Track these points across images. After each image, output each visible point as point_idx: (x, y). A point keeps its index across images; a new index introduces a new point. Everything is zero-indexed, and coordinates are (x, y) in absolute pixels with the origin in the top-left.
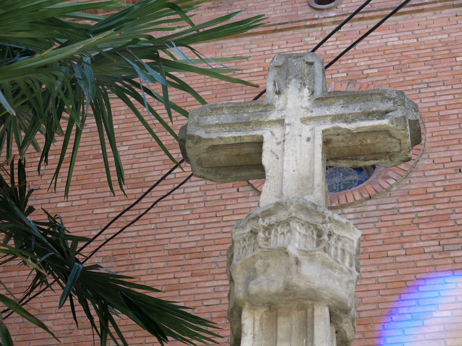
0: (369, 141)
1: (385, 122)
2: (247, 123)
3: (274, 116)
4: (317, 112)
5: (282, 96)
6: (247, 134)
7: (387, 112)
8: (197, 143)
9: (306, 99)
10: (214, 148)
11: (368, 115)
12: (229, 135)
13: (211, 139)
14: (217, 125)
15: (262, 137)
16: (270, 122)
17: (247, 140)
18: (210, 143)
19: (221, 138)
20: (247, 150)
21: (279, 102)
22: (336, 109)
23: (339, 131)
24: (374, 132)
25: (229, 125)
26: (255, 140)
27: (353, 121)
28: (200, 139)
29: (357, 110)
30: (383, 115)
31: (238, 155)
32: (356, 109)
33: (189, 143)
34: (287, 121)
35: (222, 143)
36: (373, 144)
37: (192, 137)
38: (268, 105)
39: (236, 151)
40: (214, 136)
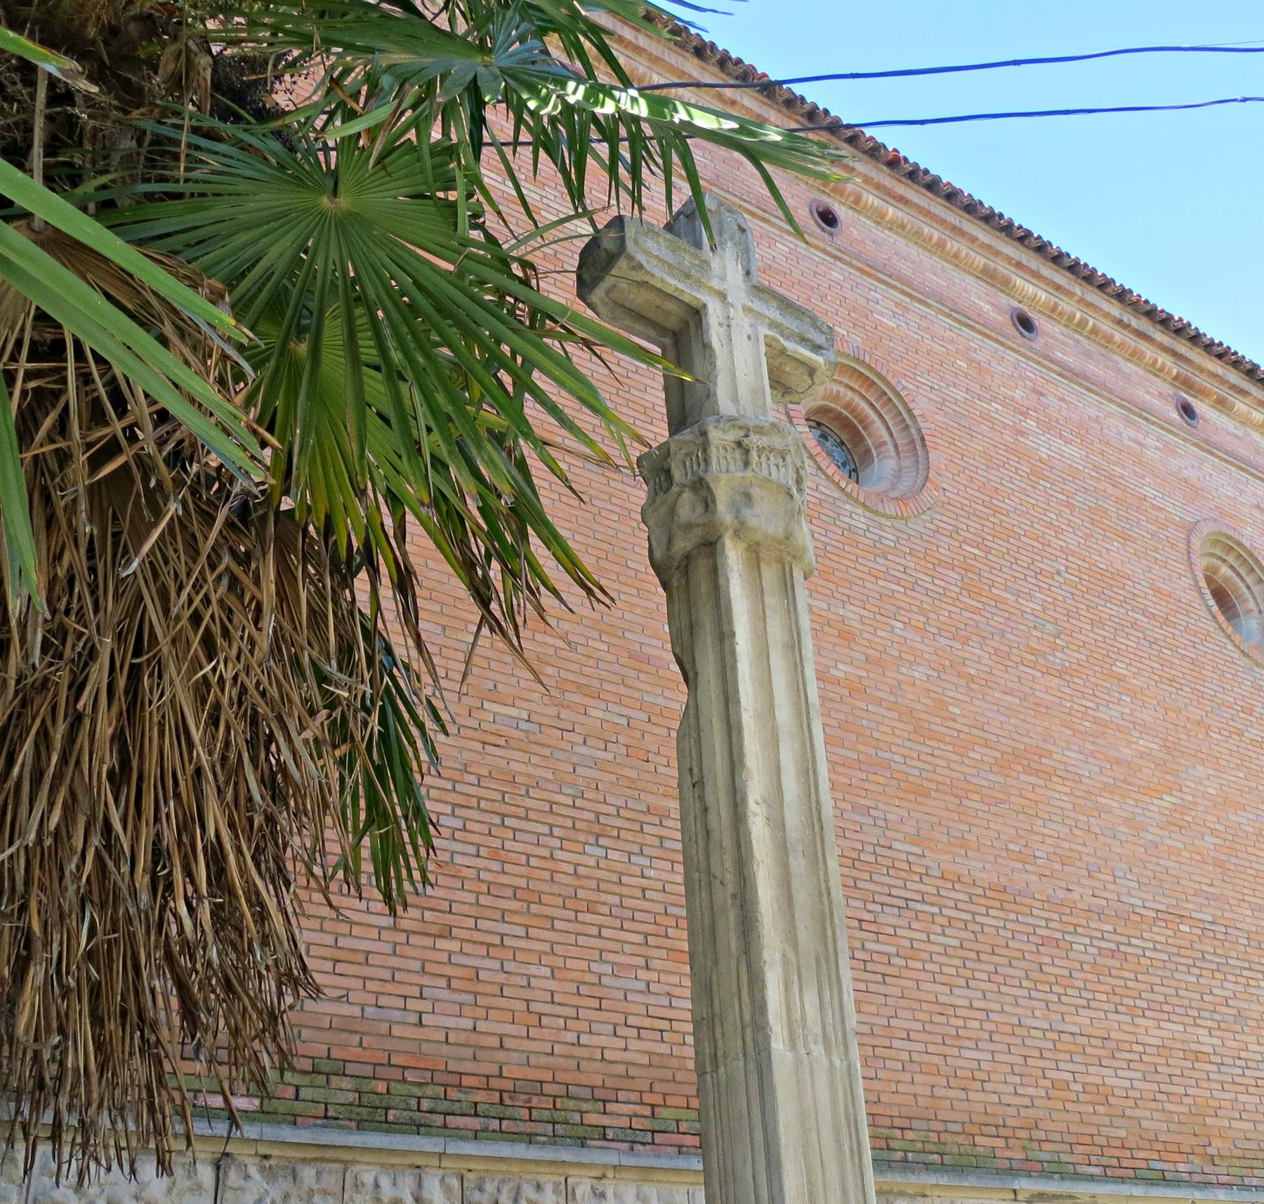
0: (788, 369)
1: (819, 359)
2: (688, 276)
3: (715, 284)
4: (757, 305)
5: (717, 259)
6: (690, 294)
7: (820, 347)
8: (633, 268)
9: (741, 278)
10: (644, 284)
11: (803, 340)
12: (673, 283)
13: (653, 276)
14: (657, 257)
15: (705, 306)
16: (711, 288)
17: (686, 299)
18: (647, 278)
19: (663, 280)
20: (671, 306)
21: (715, 264)
22: (773, 313)
23: (774, 344)
24: (802, 363)
25: (670, 265)
26: (694, 304)
27: (787, 338)
28: (641, 266)
29: (793, 327)
30: (817, 348)
31: (658, 307)
32: (792, 324)
33: (622, 263)
34: (730, 299)
35: (659, 285)
36: (789, 374)
37: (631, 258)
38: (705, 261)
39: (658, 301)
40: (658, 273)
